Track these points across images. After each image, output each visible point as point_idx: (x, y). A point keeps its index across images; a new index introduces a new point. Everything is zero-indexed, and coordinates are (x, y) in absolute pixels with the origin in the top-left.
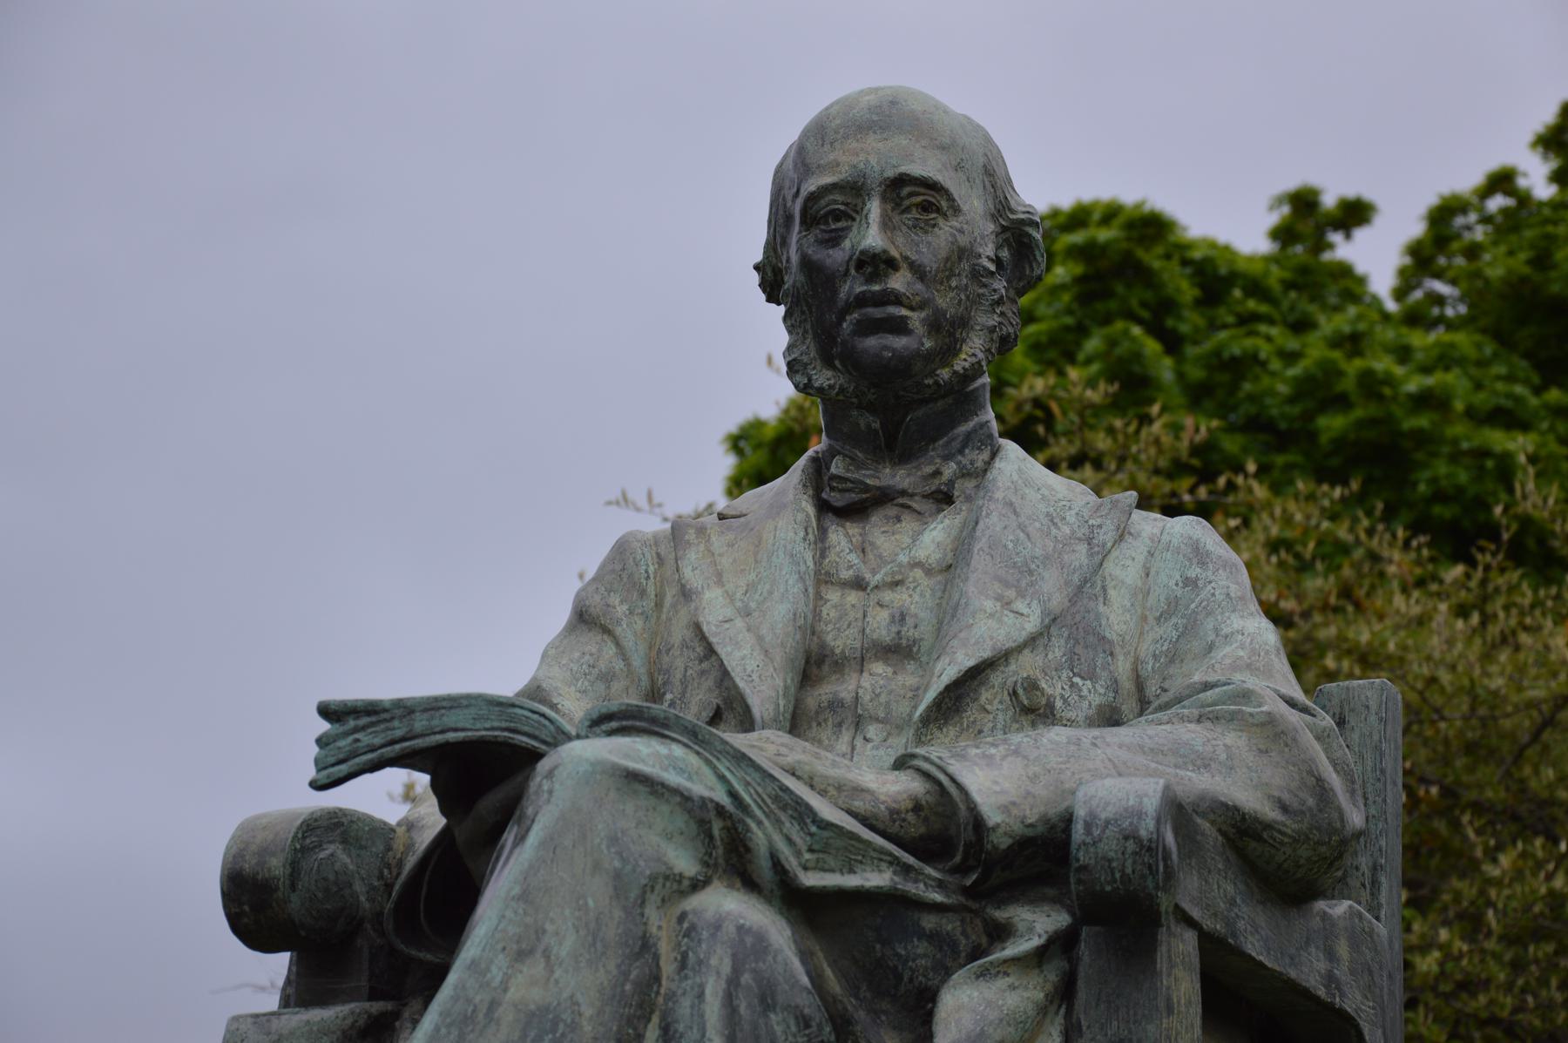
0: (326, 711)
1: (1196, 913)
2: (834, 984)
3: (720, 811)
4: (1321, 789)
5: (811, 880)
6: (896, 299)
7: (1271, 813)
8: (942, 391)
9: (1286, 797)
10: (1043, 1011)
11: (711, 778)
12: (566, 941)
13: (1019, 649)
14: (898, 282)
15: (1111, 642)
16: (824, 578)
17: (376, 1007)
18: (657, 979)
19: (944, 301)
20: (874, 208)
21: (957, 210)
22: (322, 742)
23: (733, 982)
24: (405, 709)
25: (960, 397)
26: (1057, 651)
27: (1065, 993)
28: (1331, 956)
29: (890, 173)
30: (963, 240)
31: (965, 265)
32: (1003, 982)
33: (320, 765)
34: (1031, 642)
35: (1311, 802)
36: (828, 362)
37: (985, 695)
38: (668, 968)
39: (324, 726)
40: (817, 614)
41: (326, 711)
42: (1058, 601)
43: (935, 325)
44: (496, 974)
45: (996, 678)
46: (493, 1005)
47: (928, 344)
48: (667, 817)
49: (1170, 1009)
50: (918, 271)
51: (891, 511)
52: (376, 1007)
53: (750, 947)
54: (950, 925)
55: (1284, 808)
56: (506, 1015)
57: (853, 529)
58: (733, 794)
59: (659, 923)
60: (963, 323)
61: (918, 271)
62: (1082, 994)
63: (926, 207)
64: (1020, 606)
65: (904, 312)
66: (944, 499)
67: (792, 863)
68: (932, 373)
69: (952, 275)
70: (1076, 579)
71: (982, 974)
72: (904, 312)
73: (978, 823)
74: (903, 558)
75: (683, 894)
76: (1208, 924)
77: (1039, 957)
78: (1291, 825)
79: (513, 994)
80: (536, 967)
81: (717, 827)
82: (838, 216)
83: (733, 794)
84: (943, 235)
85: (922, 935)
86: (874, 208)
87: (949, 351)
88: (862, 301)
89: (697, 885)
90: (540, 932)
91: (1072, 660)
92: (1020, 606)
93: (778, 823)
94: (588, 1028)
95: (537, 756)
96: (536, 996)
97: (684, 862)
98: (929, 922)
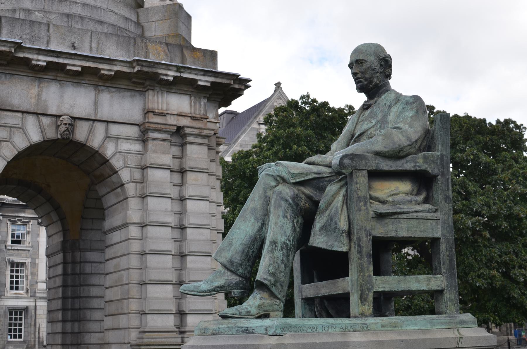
1: (364, 168)
3: (278, 176)
5: (292, 182)
6: (359, 78)
10: (341, 188)
13: (370, 128)
14: (359, 76)
15: (388, 122)
19: (367, 76)
21: (367, 62)
23: (276, 199)
34: (373, 126)
35: (391, 145)
37: (364, 137)
43: (366, 80)
45: (366, 134)
47: (366, 83)
48: (271, 178)
49: (357, 183)
50: (362, 73)
55: (385, 148)
60: (372, 77)
61: (362, 73)
63: (361, 63)
65: (361, 79)
68: (369, 86)
69: (367, 71)
70: (384, 114)
72: (361, 79)
75: (274, 188)
76: (370, 168)
79: (250, 206)
80: (253, 202)
81: (278, 178)
84: (366, 65)
85: (326, 181)
87: (370, 82)
89: (276, 186)
91: (381, 126)
92: (373, 121)
94: (259, 209)
96: (253, 206)
97: (273, 184)
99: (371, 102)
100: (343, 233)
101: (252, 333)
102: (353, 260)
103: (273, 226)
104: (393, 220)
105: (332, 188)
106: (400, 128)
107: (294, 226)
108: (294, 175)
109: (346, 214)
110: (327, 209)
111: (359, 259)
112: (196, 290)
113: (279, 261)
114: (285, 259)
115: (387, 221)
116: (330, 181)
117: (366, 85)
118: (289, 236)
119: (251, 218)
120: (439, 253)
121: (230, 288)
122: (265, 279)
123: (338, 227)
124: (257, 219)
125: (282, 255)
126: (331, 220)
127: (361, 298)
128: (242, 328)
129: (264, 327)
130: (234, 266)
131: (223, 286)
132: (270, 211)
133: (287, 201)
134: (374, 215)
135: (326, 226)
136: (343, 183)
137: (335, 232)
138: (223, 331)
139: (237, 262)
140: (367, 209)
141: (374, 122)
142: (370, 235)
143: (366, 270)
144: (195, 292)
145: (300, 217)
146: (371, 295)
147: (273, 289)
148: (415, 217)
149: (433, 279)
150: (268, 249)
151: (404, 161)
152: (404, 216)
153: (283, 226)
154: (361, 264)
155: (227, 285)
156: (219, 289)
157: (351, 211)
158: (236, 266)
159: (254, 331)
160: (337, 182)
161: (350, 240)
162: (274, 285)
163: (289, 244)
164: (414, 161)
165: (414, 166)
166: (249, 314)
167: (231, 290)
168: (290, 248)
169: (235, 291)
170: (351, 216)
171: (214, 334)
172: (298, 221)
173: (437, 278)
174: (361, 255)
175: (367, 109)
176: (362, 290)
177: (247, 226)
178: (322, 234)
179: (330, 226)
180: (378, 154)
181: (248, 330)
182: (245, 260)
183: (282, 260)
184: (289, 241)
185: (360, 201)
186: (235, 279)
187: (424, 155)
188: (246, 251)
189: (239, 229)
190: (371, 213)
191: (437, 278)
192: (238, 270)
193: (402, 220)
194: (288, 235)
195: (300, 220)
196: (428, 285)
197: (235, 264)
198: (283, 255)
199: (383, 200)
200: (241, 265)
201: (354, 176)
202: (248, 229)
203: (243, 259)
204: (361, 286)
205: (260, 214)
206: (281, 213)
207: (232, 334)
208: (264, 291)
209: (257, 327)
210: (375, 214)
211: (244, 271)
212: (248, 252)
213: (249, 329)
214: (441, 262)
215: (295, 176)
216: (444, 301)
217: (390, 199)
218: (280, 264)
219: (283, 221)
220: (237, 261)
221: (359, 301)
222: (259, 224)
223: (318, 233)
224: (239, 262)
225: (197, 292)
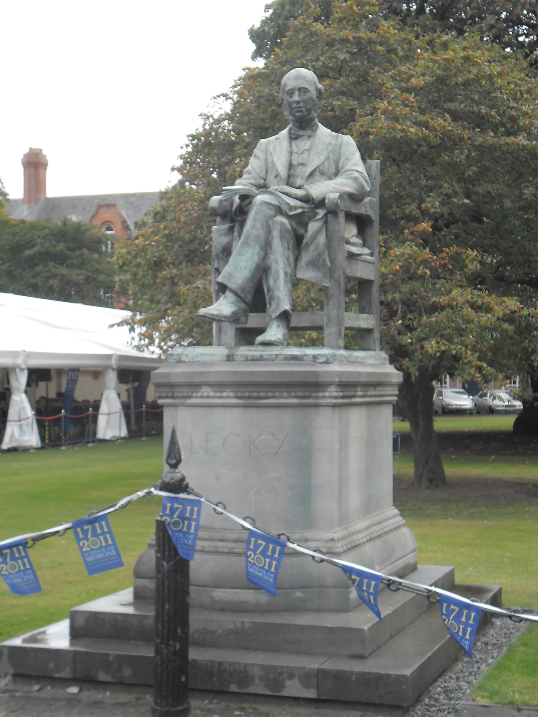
2: (294, 225)
4: (363, 187)
7: (355, 192)
10: (323, 225)
12: (259, 225)
14: (301, 105)
16: (291, 153)
17: (232, 224)
19: (308, 106)
25: (312, 120)
27: (326, 222)
36: (291, 115)
51: (301, 138)
52: (232, 224)
53: (283, 224)
54: (310, 214)
55: (357, 191)
57: (296, 142)
58: (280, 203)
59: (270, 222)
61: (304, 102)
63: (305, 92)
66: (310, 137)
67: (288, 211)
71: (315, 221)
74: (303, 149)
77: (322, 218)
82: (291, 93)
83: (280, 203)
84: (308, 95)
86: (297, 93)
88: (296, 108)
89: (275, 216)
95: (254, 197)
99: (301, 133)
101: (302, 360)
106: (362, 173)
136: (324, 219)
138: (267, 357)
165: (366, 211)
187: (370, 199)
190: (346, 254)
193: (360, 263)
196: (368, 323)
197: (245, 291)
206: (286, 245)
217: (352, 240)
223: (305, 267)
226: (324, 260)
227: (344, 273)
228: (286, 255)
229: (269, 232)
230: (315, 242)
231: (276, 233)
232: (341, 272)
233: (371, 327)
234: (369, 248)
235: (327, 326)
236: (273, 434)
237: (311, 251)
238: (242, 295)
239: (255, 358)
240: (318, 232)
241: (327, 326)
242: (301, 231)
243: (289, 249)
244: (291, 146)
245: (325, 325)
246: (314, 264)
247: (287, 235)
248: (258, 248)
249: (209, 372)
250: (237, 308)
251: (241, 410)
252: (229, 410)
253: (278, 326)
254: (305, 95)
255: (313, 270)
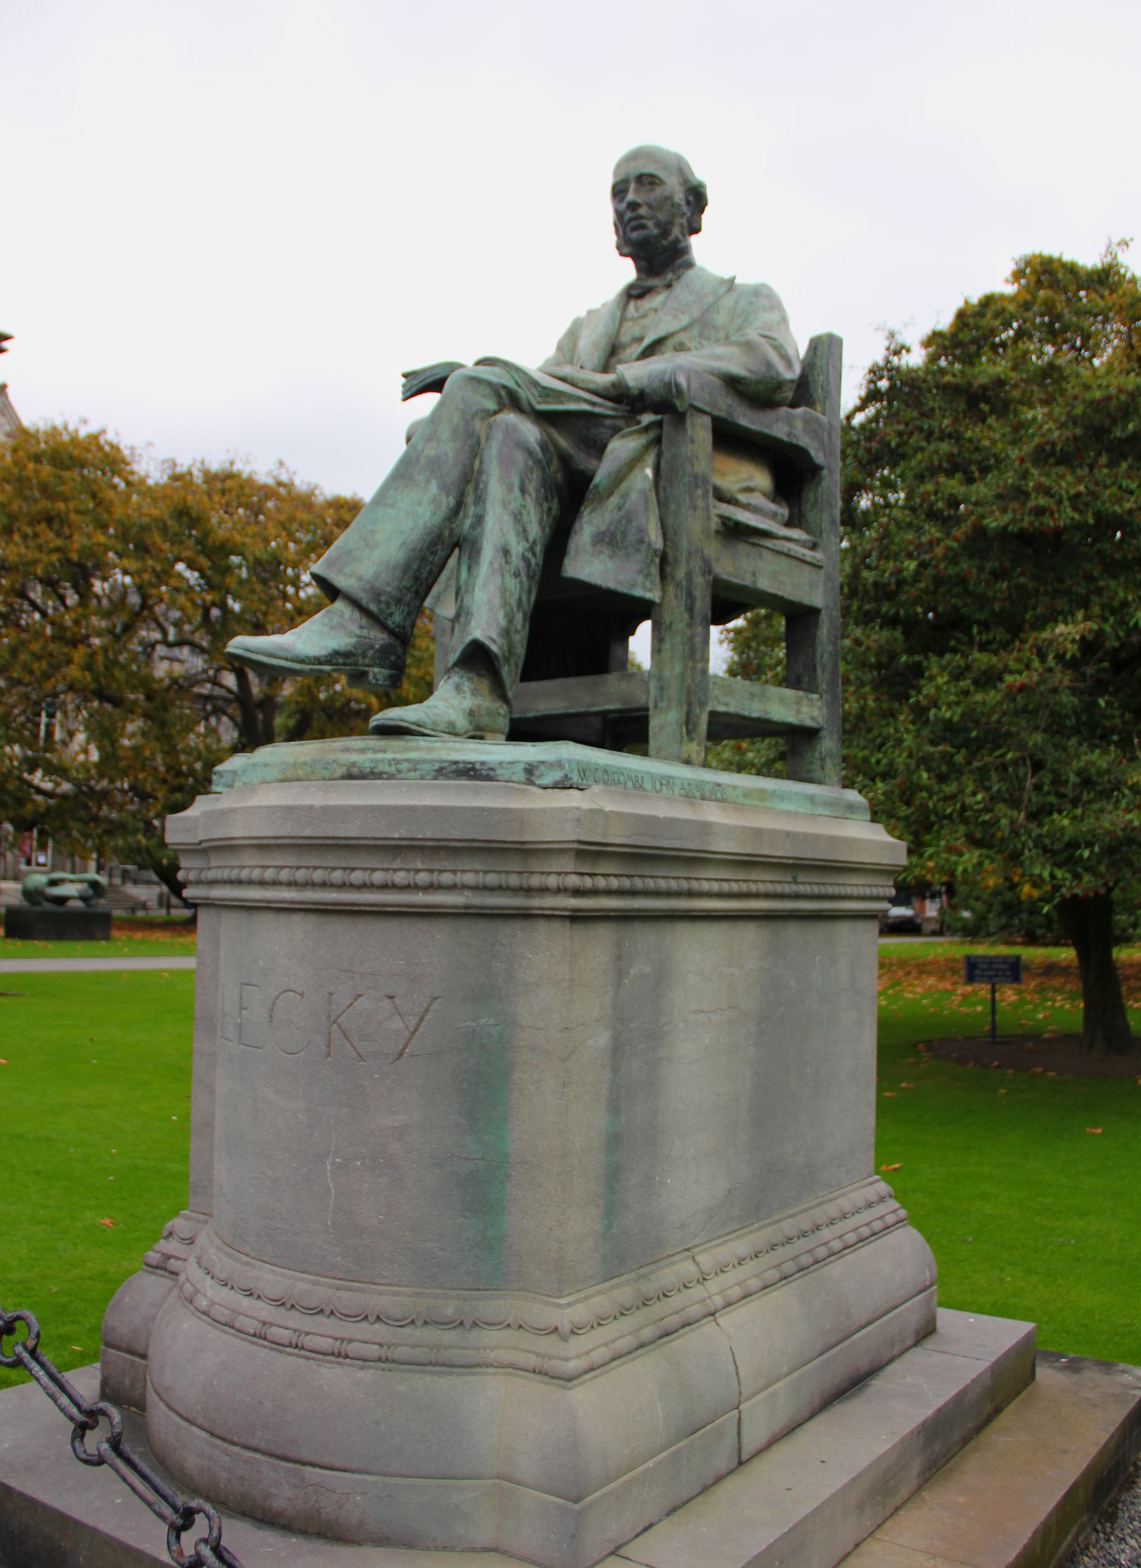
0: (405, 376)
1: (707, 409)
3: (504, 387)
4: (769, 365)
6: (641, 217)
8: (665, 249)
9: (752, 368)
10: (646, 448)
11: (508, 376)
13: (678, 332)
14: (643, 211)
16: (623, 320)
18: (479, 443)
19: (662, 216)
20: (632, 186)
21: (662, 182)
22: (404, 386)
24: (424, 371)
26: (695, 331)
27: (658, 441)
28: (791, 426)
29: (637, 173)
30: (667, 193)
31: (669, 203)
32: (630, 438)
33: (404, 393)
34: (684, 329)
37: (663, 349)
38: (483, 440)
39: (404, 380)
40: (618, 331)
41: (405, 376)
42: (696, 314)
43: (658, 225)
44: (420, 447)
46: (418, 457)
49: (692, 441)
50: (649, 206)
54: (618, 423)
56: (422, 460)
58: (516, 383)
61: (649, 206)
62: (664, 440)
63: (651, 184)
64: (681, 317)
67: (534, 402)
71: (624, 436)
73: (628, 388)
76: (716, 413)
77: (647, 429)
78: (753, 377)
81: (503, 393)
83: (516, 383)
84: (659, 192)
85: (604, 426)
86: (632, 186)
89: (495, 413)
90: (436, 432)
93: (529, 389)
97: (491, 405)
98: (608, 422)
100: (656, 555)
101: (489, 778)
102: (670, 625)
103: (499, 509)
104: (749, 547)
105: (621, 447)
107: (542, 519)
108: (547, 393)
109: (657, 512)
110: (610, 494)
111: (689, 625)
112: (283, 654)
113: (514, 603)
114: (524, 598)
115: (742, 548)
116: (616, 430)
117: (656, 237)
118: (534, 542)
119: (428, 482)
120: (813, 646)
121: (367, 661)
122: (494, 641)
123: (646, 539)
124: (444, 488)
125: (518, 586)
126: (629, 520)
127: (687, 723)
128: (456, 763)
129: (523, 766)
130: (380, 602)
131: (350, 652)
132: (481, 472)
133: (530, 453)
134: (721, 528)
135: (613, 535)
136: (652, 435)
137: (638, 551)
138: (387, 769)
139: (390, 593)
140: (708, 509)
141: (685, 320)
142: (710, 572)
143: (698, 656)
144: (280, 658)
145: (556, 500)
146: (704, 718)
147: (505, 671)
148: (786, 551)
149: (805, 701)
150: (491, 563)
151: (771, 415)
152: (769, 543)
153: (521, 514)
154: (691, 638)
155: (360, 651)
156: (341, 660)
157: (673, 507)
158: (388, 604)
159: (492, 773)
160: (639, 432)
161: (663, 575)
162: (507, 660)
163: (533, 562)
164: (790, 421)
165: (789, 434)
166: (451, 730)
167: (369, 666)
168: (535, 574)
169: (376, 670)
170: (670, 521)
171: (350, 776)
172: (550, 509)
173: (811, 700)
174: (692, 617)
175: (640, 296)
176: (690, 704)
177: (419, 503)
178: (601, 552)
179: (624, 534)
180: (732, 383)
181: (473, 769)
182: (409, 589)
183: (520, 601)
184: (534, 554)
185: (697, 487)
186: (379, 638)
187: (805, 412)
188: (415, 566)
189: (392, 506)
190: (715, 523)
191: (811, 700)
192: (391, 614)
193: (765, 553)
194: (531, 539)
195: (555, 506)
196: (798, 712)
198: (521, 588)
199: (729, 496)
200: (399, 601)
201: (688, 422)
202: (420, 510)
203: (405, 587)
204: (689, 694)
205: (453, 475)
206: (516, 481)
207: (422, 778)
208: (480, 675)
209: (501, 763)
210: (724, 524)
211: (405, 619)
212: (419, 570)
213: (478, 766)
214: (818, 666)
215: (547, 396)
216: (817, 754)
217: (742, 498)
218: (515, 609)
219: (520, 500)
220: (389, 589)
221: (684, 729)
222: (452, 501)
223: (589, 548)
224: (394, 593)
225: (287, 659)
226: (641, 530)
227: (707, 570)
228: (514, 506)
229: (475, 449)
230: (624, 486)
231: (493, 451)
232: (697, 565)
233: (808, 723)
234: (808, 531)
235: (656, 707)
236: (391, 997)
237: (610, 508)
238: (373, 607)
239: (355, 771)
240: (634, 462)
241: (656, 707)
242: (583, 461)
243: (523, 490)
244: (625, 308)
245: (651, 705)
246: (609, 540)
247: (520, 457)
248: (434, 488)
249: (238, 809)
250: (353, 640)
251: (312, 921)
252: (283, 918)
253: (458, 688)
254: (652, 190)
255: (611, 557)
